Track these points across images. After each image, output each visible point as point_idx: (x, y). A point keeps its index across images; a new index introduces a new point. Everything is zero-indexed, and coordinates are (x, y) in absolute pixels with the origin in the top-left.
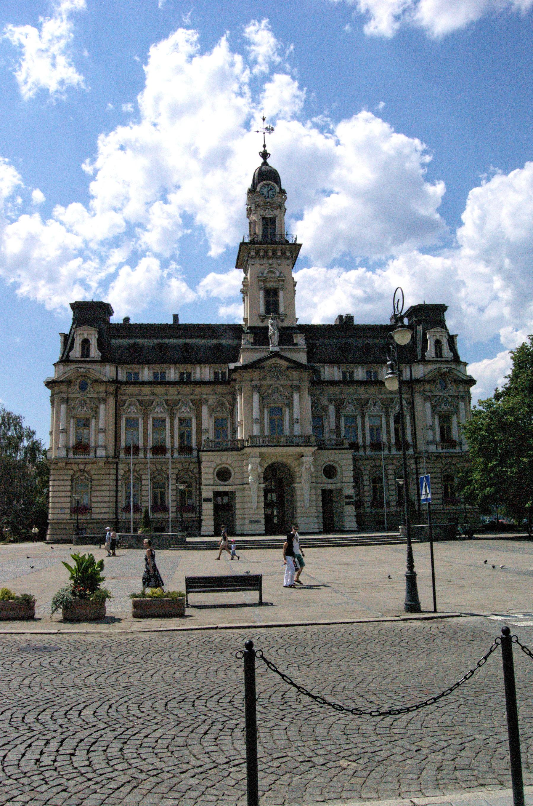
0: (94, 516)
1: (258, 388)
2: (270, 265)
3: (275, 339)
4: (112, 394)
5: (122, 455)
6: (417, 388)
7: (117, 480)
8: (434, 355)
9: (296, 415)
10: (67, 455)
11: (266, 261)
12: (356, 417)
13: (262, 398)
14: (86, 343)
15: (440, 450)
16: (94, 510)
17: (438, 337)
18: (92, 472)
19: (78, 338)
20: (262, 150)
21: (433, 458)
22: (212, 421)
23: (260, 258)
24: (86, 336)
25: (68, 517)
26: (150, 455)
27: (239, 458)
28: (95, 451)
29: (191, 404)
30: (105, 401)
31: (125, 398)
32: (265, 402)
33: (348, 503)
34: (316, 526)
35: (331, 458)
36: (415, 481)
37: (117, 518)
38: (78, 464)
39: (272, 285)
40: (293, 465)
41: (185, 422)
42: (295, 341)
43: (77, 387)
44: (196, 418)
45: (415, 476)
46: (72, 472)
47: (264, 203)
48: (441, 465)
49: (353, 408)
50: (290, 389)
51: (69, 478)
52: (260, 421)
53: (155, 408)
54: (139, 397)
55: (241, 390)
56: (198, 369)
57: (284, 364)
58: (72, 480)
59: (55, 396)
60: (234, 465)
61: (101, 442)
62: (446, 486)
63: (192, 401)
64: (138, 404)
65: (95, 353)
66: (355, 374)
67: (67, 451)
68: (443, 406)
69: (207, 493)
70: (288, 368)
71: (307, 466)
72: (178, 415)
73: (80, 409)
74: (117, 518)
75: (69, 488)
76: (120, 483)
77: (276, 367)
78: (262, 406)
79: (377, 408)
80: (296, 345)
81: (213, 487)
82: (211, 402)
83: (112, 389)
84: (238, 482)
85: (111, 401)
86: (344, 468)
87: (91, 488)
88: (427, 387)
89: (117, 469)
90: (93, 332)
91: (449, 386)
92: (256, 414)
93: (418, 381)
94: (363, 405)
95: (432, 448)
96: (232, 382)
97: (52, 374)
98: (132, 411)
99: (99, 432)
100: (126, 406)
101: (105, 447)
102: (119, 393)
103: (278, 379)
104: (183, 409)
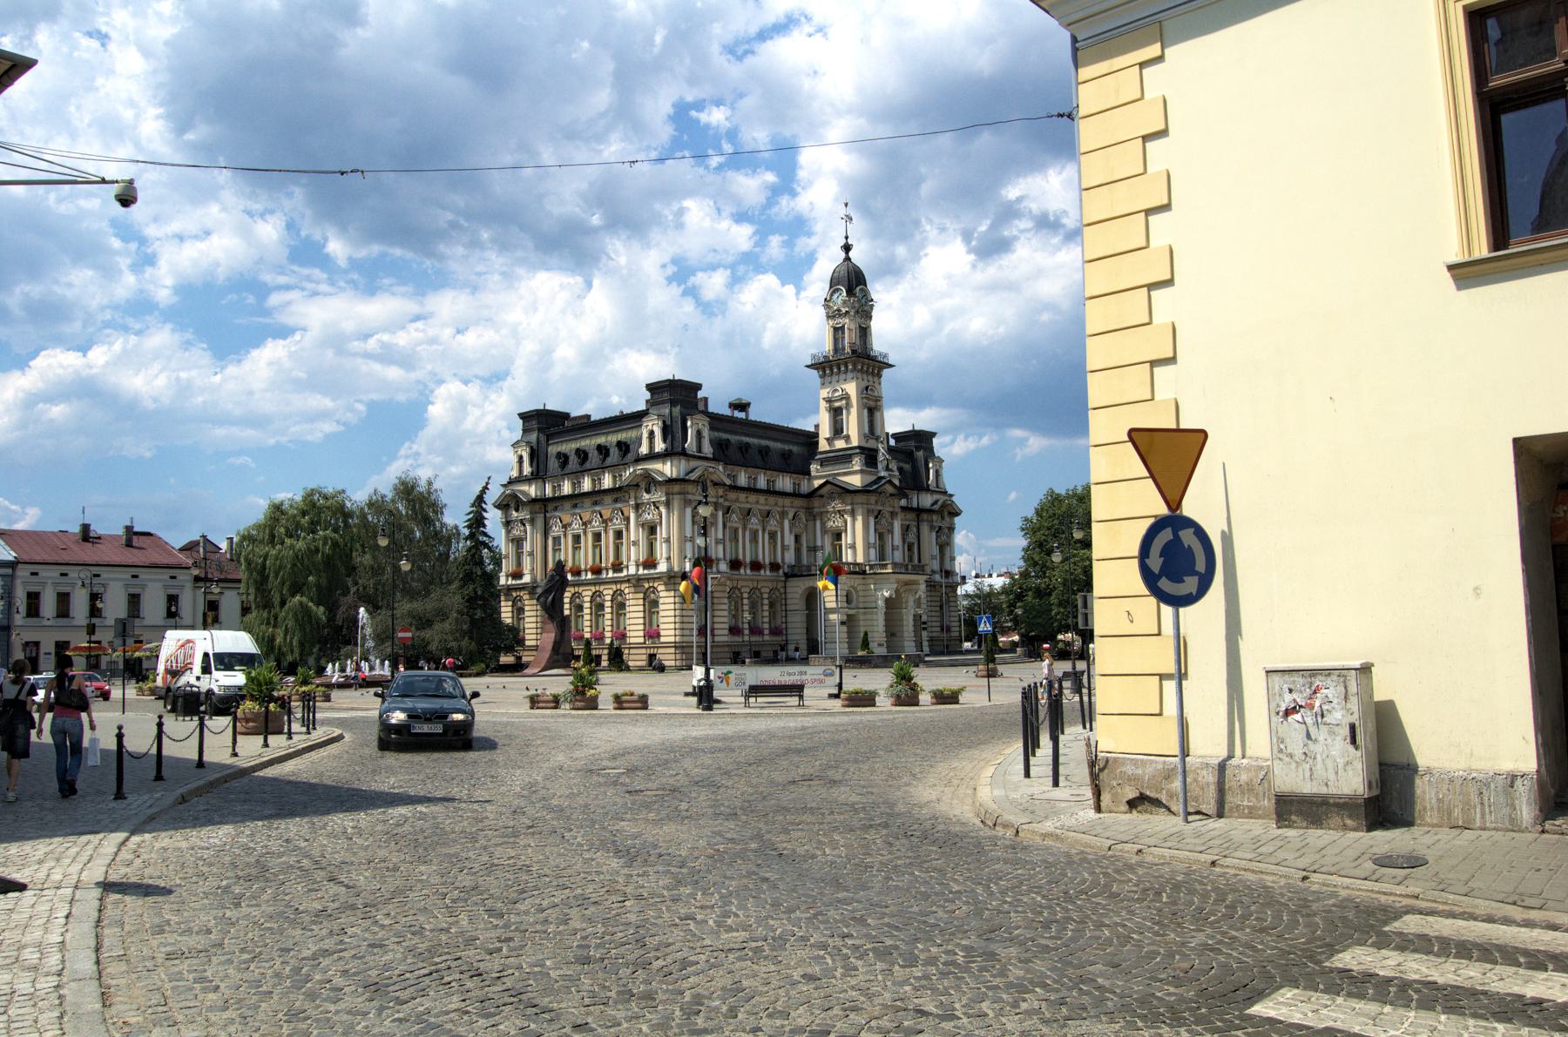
6: (925, 516)
39: (872, 404)
65: (708, 449)
82: (791, 516)
88: (935, 517)
92: (872, 540)
93: (929, 511)
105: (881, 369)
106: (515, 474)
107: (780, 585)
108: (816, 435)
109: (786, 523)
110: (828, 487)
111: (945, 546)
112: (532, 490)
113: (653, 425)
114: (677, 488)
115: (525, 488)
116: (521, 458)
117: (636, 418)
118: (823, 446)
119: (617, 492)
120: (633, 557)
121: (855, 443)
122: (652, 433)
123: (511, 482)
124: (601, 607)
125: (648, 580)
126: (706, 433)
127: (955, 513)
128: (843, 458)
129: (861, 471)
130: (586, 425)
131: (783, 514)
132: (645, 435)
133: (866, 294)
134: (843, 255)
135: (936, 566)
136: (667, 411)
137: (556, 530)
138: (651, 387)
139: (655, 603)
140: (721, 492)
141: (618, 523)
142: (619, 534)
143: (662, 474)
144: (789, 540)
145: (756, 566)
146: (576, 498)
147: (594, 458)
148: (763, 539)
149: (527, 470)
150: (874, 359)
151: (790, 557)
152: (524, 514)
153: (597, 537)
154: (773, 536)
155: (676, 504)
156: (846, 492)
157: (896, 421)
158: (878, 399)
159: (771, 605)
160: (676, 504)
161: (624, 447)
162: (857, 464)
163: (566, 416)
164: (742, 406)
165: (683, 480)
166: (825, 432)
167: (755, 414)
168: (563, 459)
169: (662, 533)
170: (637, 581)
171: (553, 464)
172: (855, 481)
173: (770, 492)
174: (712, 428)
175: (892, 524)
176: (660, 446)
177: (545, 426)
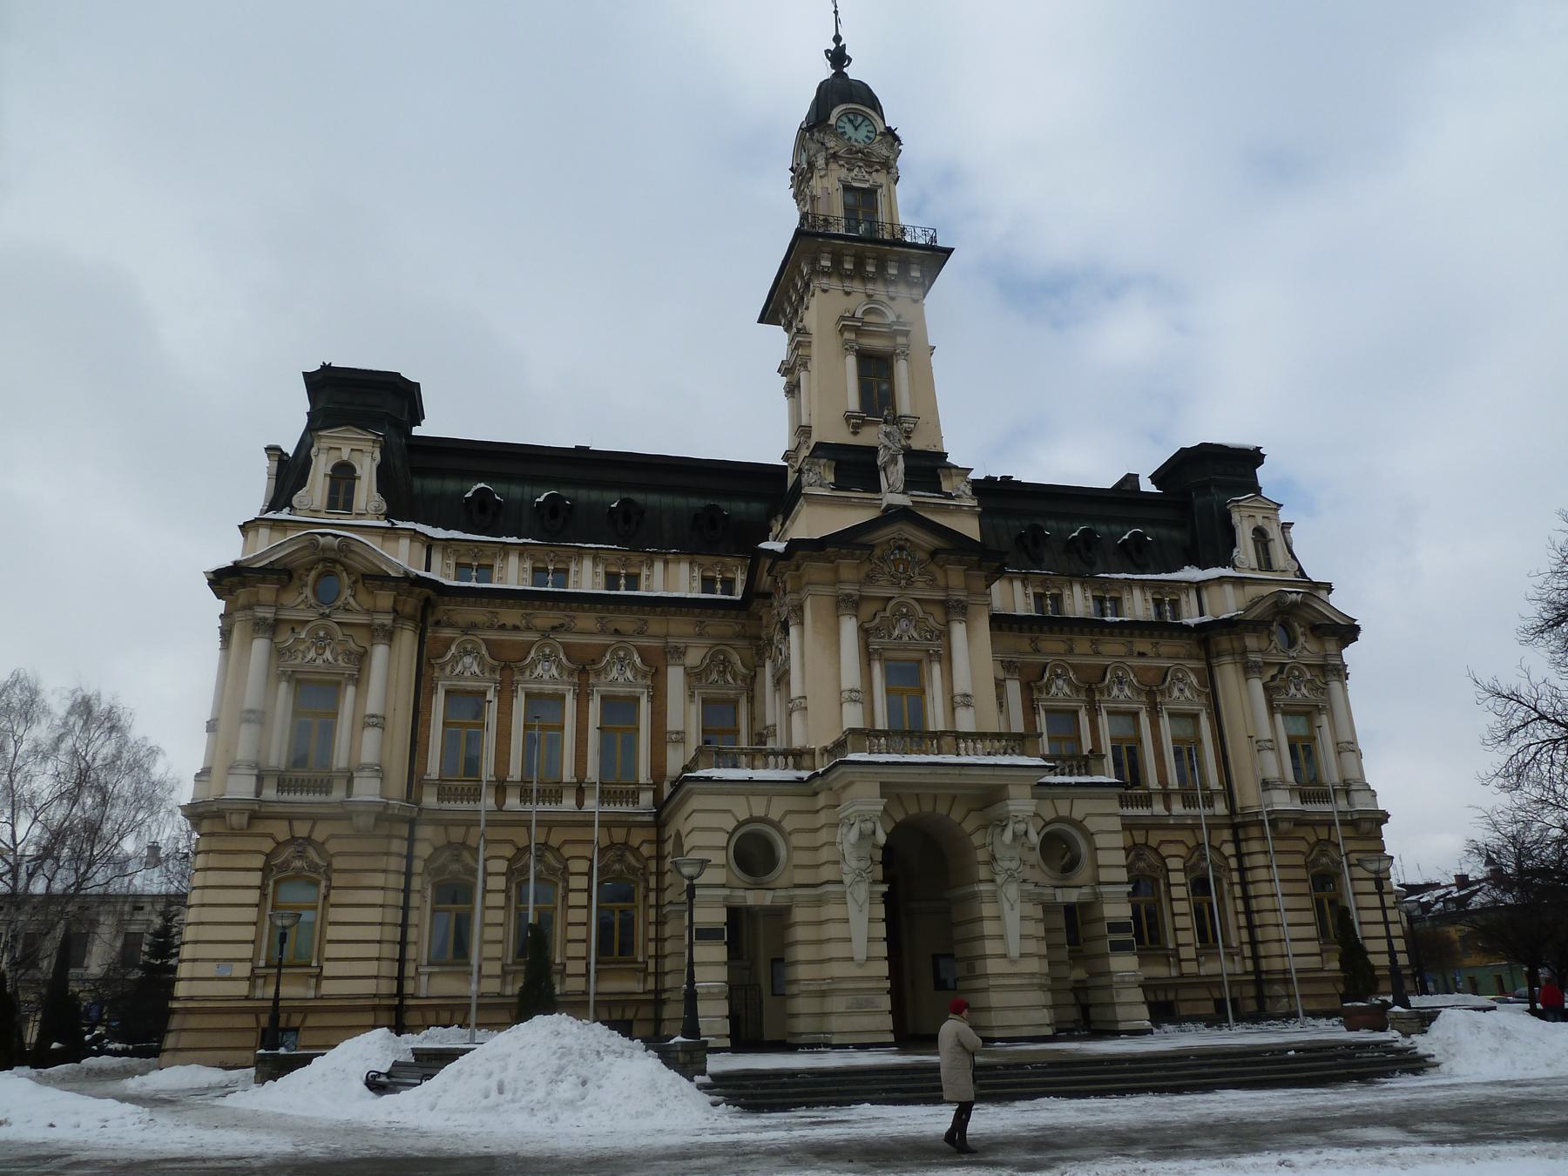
0: (328, 988)
1: (852, 604)
2: (869, 296)
3: (895, 474)
4: (412, 618)
5: (430, 800)
6: (1224, 643)
7: (408, 874)
8: (1255, 565)
9: (962, 684)
10: (258, 793)
11: (857, 286)
12: (1075, 713)
13: (865, 633)
14: (343, 475)
15: (1297, 805)
16: (329, 969)
17: (1260, 522)
18: (332, 847)
19: (323, 458)
20: (832, 46)
21: (1284, 826)
22: (695, 710)
23: (844, 276)
24: (345, 455)
25: (242, 988)
28: (350, 781)
29: (638, 661)
30: (389, 635)
31: (447, 633)
32: (875, 643)
33: (1118, 947)
34: (1044, 1016)
35: (1064, 812)
36: (1238, 890)
37: (400, 993)
38: (290, 819)
40: (968, 826)
41: (619, 709)
42: (946, 486)
43: (308, 592)
44: (652, 699)
45: (1236, 877)
46: (268, 846)
47: (850, 151)
48: (1303, 846)
49: (1066, 689)
50: (938, 612)
51: (259, 861)
52: (864, 696)
53: (534, 664)
54: (493, 635)
56: (659, 566)
57: (927, 540)
58: (266, 870)
59: (238, 616)
60: (788, 824)
61: (368, 754)
62: (1319, 903)
63: (642, 652)
64: (484, 651)
66: (1067, 602)
67: (260, 779)
68: (1293, 691)
69: (711, 915)
70: (933, 554)
71: (1022, 827)
72: (601, 687)
73: (312, 654)
74: (400, 993)
75: (254, 896)
76: (416, 883)
77: (901, 548)
78: (868, 655)
79: (1127, 691)
80: (949, 496)
81: (726, 892)
82: (694, 657)
83: (410, 605)
84: (801, 877)
85: (407, 640)
86: (1100, 841)
87: (326, 897)
88: (1251, 642)
89: (411, 840)
90: (367, 447)
91: (1301, 639)
92: (851, 675)
93: (1230, 625)
94: (1091, 685)
95: (1283, 801)
96: (756, 604)
97: (230, 550)
98: (468, 670)
99: (366, 725)
100: (449, 655)
101: (380, 772)
102: (431, 620)
103: (910, 582)
104: (614, 673)
126: (367, 470)
135: (1277, 765)
144: (683, 714)
162: (818, 481)
172: (810, 523)
175: (946, 634)
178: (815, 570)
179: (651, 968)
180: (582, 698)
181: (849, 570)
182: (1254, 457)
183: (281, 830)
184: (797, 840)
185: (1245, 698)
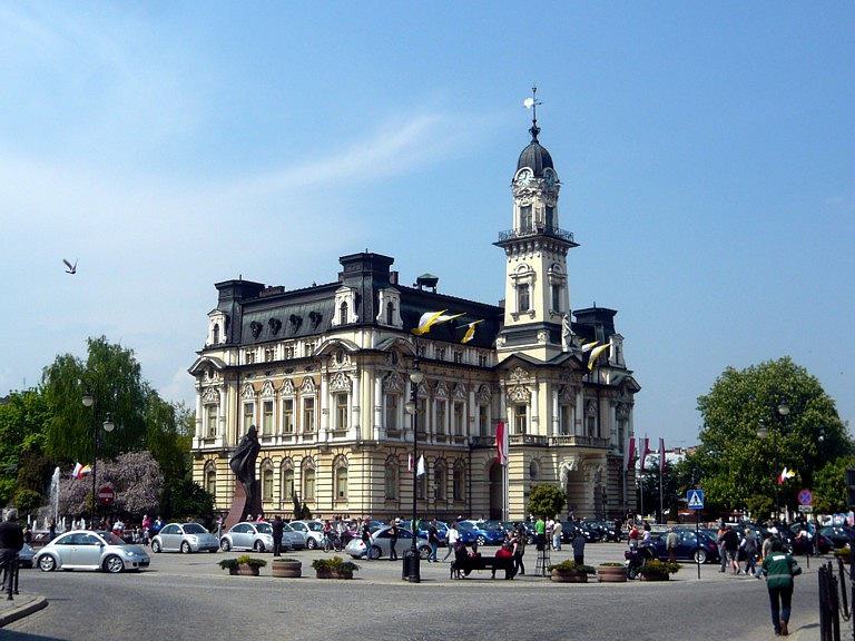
0: (402, 507)
11: (551, 254)
25: (383, 507)
26: (435, 442)
27: (544, 454)
39: (557, 281)
55: (537, 387)
65: (398, 321)
105: (566, 248)
106: (210, 342)
107: (465, 456)
108: (501, 310)
109: (472, 395)
110: (513, 362)
111: (624, 419)
112: (227, 358)
113: (345, 296)
114: (367, 359)
115: (219, 355)
116: (217, 326)
117: (332, 289)
118: (509, 321)
119: (309, 362)
120: (323, 425)
121: (540, 318)
122: (344, 304)
123: (207, 349)
124: (290, 472)
125: (338, 447)
126: (397, 306)
127: (635, 389)
128: (527, 333)
129: (546, 346)
130: (279, 296)
131: (469, 387)
132: (338, 307)
133: (551, 173)
134: (531, 138)
135: (615, 440)
136: (360, 284)
137: (248, 398)
138: (345, 261)
139: (343, 470)
140: (410, 364)
141: (308, 392)
142: (309, 402)
143: (354, 344)
144: (475, 412)
145: (441, 437)
146: (269, 367)
147: (287, 328)
148: (450, 410)
149: (222, 338)
150: (558, 238)
151: (475, 429)
152: (218, 380)
153: (288, 404)
154: (459, 408)
155: (366, 375)
156: (531, 366)
157: (580, 298)
158: (563, 277)
159: (456, 475)
160: (366, 375)
161: (317, 318)
162: (542, 337)
163: (261, 287)
164: (432, 282)
165: (374, 351)
166: (511, 306)
167: (441, 289)
168: (257, 327)
169: (352, 402)
170: (326, 449)
171: (248, 333)
172: (540, 354)
173: (456, 365)
174: (402, 302)
176: (352, 318)
177: (242, 294)
178: (544, 373)
179: (468, 501)
180: (450, 402)
181: (557, 374)
182: (614, 312)
183: (388, 451)
184: (544, 466)
185: (609, 414)
